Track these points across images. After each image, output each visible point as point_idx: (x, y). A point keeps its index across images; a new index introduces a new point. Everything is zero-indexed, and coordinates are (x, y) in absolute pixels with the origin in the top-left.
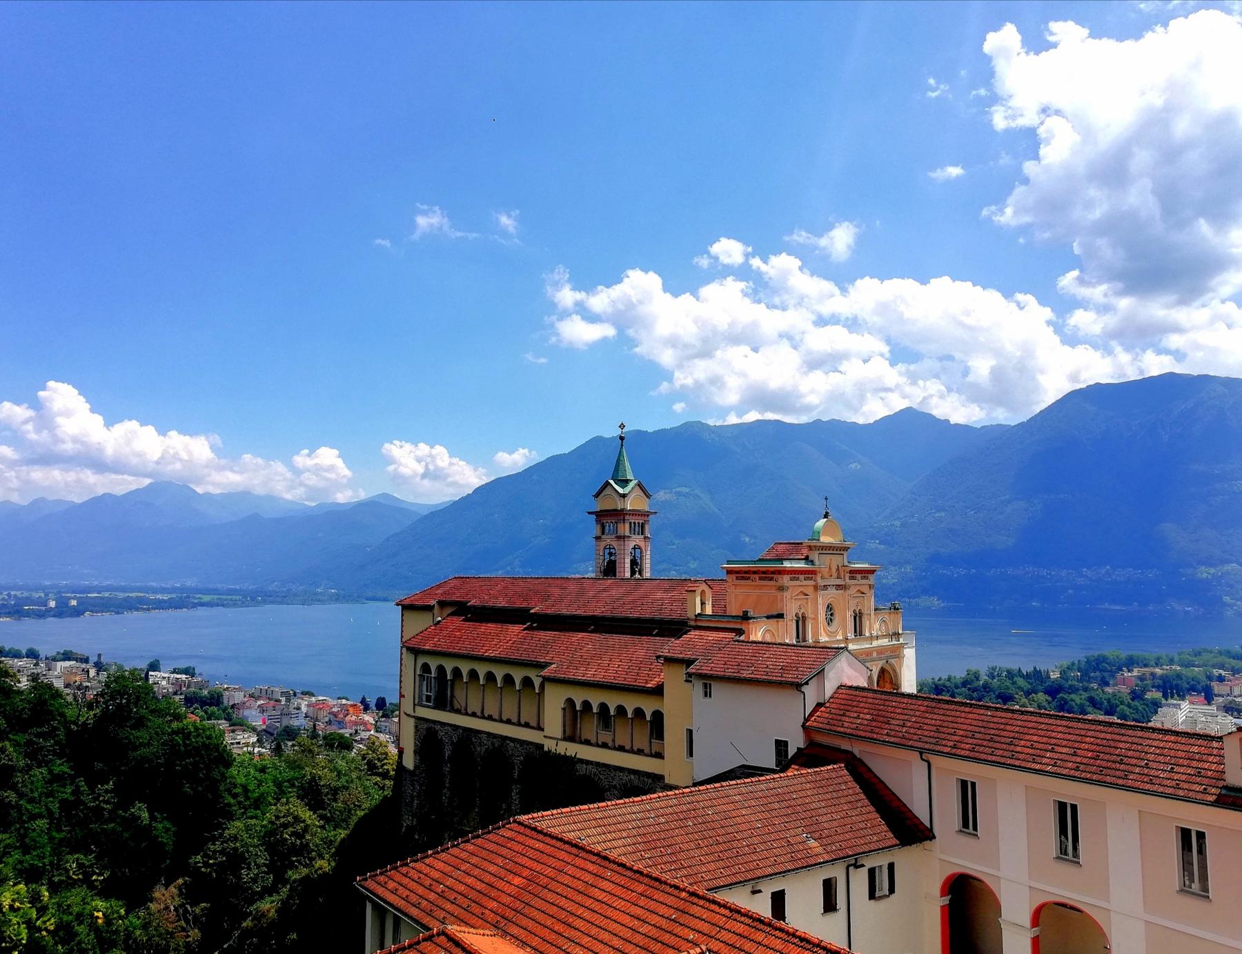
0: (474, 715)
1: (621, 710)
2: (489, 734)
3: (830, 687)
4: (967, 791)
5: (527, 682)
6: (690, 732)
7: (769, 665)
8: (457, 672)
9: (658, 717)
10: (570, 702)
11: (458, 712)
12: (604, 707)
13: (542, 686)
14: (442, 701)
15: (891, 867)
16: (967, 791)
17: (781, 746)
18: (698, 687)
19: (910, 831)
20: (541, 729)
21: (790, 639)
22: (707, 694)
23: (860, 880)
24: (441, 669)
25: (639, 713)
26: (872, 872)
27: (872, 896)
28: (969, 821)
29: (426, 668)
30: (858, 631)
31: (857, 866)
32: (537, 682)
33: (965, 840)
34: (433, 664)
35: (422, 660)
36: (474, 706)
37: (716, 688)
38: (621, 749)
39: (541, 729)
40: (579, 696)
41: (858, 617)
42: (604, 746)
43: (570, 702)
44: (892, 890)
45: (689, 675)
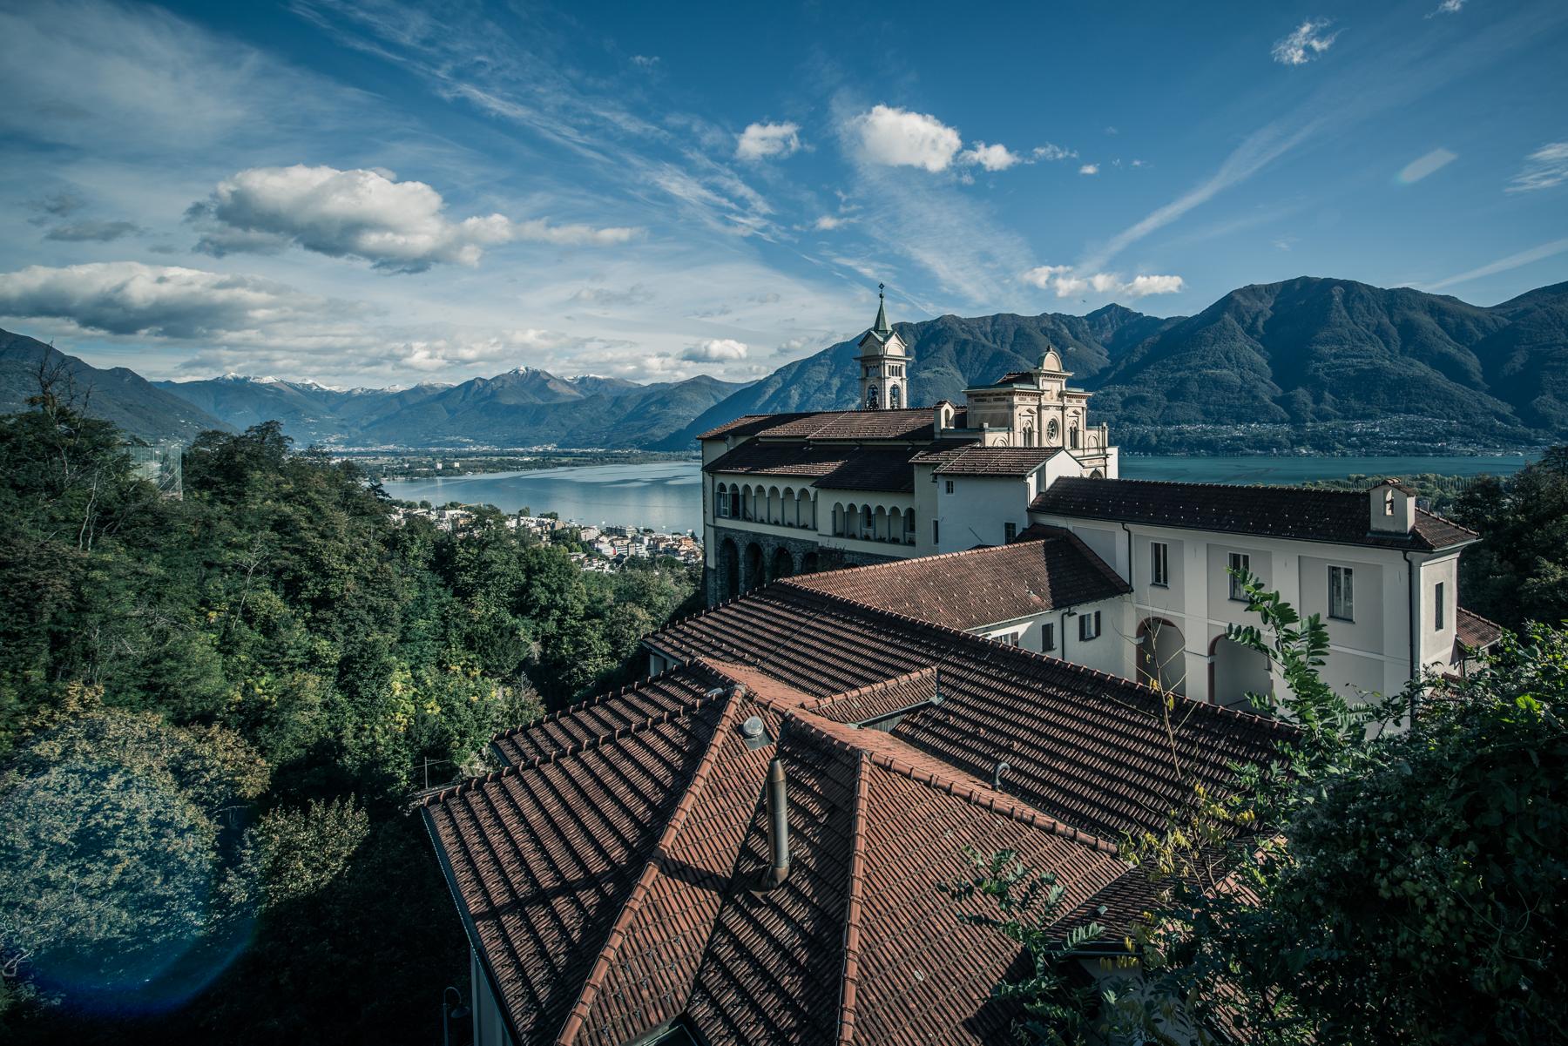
0: (762, 521)
1: (880, 509)
2: (775, 537)
3: (1050, 481)
4: (1160, 554)
5: (804, 492)
6: (936, 523)
7: (1002, 463)
8: (747, 487)
9: (911, 512)
10: (838, 505)
11: (749, 520)
12: (867, 509)
13: (816, 495)
14: (735, 515)
15: (1098, 615)
16: (1159, 553)
17: (1010, 527)
18: (942, 483)
19: (1112, 586)
20: (815, 529)
21: (1020, 442)
22: (949, 490)
23: (1072, 625)
24: (734, 487)
25: (895, 510)
26: (1082, 618)
27: (1082, 638)
28: (1161, 578)
29: (722, 487)
30: (1075, 445)
31: (1071, 614)
32: (812, 491)
33: (1157, 590)
34: (728, 482)
35: (720, 480)
36: (762, 512)
37: (959, 485)
38: (882, 540)
39: (815, 529)
40: (845, 500)
41: (1074, 432)
42: (867, 538)
43: (838, 505)
44: (1098, 633)
45: (936, 475)
